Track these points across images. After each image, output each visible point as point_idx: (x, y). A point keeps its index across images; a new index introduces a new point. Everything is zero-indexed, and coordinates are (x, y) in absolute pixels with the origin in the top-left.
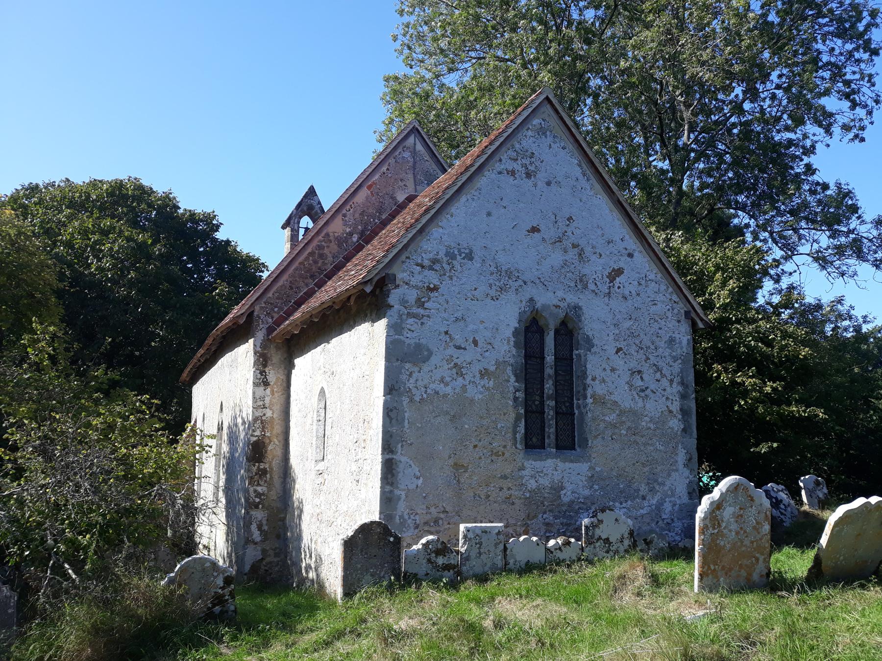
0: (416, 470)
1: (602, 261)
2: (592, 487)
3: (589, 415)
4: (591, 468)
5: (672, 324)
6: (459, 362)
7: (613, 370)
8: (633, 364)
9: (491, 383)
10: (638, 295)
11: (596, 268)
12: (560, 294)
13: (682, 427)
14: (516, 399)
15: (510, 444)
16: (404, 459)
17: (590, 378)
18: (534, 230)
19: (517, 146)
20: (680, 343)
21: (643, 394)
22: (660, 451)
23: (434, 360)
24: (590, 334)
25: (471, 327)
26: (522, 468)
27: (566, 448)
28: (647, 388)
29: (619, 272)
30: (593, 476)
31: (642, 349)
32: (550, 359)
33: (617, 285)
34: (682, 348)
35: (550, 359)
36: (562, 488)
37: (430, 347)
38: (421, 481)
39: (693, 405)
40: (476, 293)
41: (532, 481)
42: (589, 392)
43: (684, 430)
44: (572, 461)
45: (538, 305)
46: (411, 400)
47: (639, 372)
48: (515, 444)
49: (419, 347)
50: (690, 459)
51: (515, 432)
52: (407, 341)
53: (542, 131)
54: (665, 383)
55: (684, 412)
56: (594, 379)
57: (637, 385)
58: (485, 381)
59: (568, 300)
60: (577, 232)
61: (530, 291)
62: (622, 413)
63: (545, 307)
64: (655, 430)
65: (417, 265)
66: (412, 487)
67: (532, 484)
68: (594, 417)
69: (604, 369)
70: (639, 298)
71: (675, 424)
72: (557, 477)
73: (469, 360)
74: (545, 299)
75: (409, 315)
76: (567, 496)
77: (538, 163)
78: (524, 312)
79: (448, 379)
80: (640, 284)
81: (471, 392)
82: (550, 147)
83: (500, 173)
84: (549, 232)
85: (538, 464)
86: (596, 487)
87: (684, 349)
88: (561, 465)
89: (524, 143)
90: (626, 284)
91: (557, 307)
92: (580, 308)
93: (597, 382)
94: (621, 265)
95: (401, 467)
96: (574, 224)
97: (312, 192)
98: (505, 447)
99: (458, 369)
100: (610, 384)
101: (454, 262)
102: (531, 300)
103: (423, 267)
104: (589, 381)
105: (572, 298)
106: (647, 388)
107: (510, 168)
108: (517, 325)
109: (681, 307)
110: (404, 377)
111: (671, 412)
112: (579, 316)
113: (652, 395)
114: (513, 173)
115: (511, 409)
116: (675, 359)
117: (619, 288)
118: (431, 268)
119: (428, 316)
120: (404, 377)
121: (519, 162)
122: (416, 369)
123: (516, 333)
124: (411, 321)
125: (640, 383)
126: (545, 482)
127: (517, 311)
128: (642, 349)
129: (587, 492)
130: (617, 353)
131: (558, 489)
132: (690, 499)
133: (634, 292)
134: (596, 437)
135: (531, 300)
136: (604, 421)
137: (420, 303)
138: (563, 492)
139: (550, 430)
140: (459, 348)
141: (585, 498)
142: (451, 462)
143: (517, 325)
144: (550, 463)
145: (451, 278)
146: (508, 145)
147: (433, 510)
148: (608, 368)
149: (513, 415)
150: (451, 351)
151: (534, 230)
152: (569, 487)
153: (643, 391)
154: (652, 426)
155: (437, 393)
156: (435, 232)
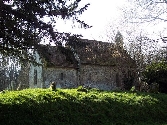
68: (37, 80)
71: (41, 80)
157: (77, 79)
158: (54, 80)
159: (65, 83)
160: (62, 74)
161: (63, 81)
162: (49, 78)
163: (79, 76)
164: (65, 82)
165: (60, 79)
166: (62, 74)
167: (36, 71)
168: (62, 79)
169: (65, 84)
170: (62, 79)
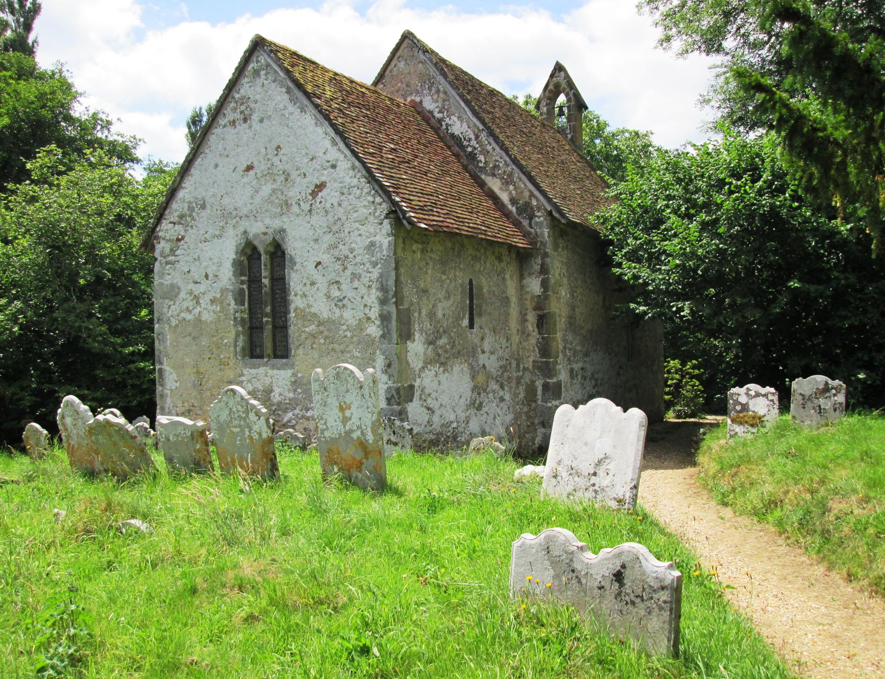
0: (175, 376)
1: (306, 180)
2: (295, 391)
3: (292, 327)
4: (294, 375)
6: (196, 293)
7: (313, 284)
8: (332, 276)
9: (218, 308)
10: (340, 205)
11: (300, 189)
12: (268, 221)
13: (381, 333)
14: (235, 319)
15: (232, 355)
16: (168, 368)
17: (293, 293)
18: (249, 168)
19: (237, 96)
20: (381, 246)
21: (340, 304)
22: (357, 358)
23: (182, 295)
24: (293, 253)
25: (205, 264)
26: (242, 375)
27: (282, 357)
28: (344, 298)
29: (321, 187)
30: (296, 381)
31: (339, 259)
32: (266, 281)
33: (318, 201)
34: (381, 252)
35: (266, 281)
36: (272, 391)
37: (179, 284)
38: (178, 385)
39: (393, 309)
40: (207, 236)
41: (249, 385)
42: (292, 307)
43: (383, 336)
44: (278, 369)
45: (251, 236)
46: (171, 327)
47: (337, 282)
48: (236, 355)
49: (172, 285)
51: (236, 346)
52: (166, 283)
53: (256, 73)
54: (363, 290)
55: (384, 318)
56: (296, 295)
57: (335, 295)
58: (214, 307)
59: (275, 226)
60: (284, 158)
61: (245, 225)
62: (320, 324)
63: (256, 236)
64: (352, 337)
65: (171, 223)
66: (174, 388)
69: (305, 284)
70: (340, 209)
71: (374, 330)
72: (268, 381)
73: (203, 291)
74: (256, 228)
75: (167, 263)
77: (252, 105)
78: (240, 244)
79: (191, 308)
80: (343, 194)
81: (207, 317)
82: (263, 85)
83: (225, 126)
84: (261, 167)
85: (253, 371)
86: (299, 390)
87: (385, 253)
88: (270, 372)
89: (242, 91)
90: (328, 198)
91: (265, 234)
92: (284, 231)
93: (298, 297)
94: (323, 179)
95: (167, 374)
96: (282, 152)
97: (559, 68)
98: (229, 358)
99: (197, 299)
100: (310, 298)
101: (194, 214)
102: (245, 232)
103: (174, 223)
104: (292, 297)
105: (276, 224)
106: (344, 298)
107: (231, 119)
108: (235, 257)
109: (385, 207)
110: (165, 310)
111: (369, 319)
112: (283, 239)
113: (349, 304)
114: (233, 123)
115: (232, 328)
116: (374, 264)
117: (321, 202)
118: (180, 223)
119: (178, 261)
120: (165, 310)
121: (238, 111)
122: (172, 302)
124: (168, 267)
127: (235, 244)
128: (339, 259)
129: (291, 395)
130: (316, 267)
131: (269, 391)
132: (389, 404)
133: (335, 204)
134: (297, 348)
135: (245, 232)
136: (304, 332)
137: (173, 252)
138: (272, 394)
140: (196, 283)
141: (290, 400)
142: (195, 370)
143: (235, 257)
144: (262, 370)
145: (192, 227)
146: (229, 99)
147: (186, 404)
148: (308, 286)
149: (234, 333)
150: (191, 286)
151: (249, 168)
152: (277, 390)
153: (341, 300)
154: (349, 334)
155: (184, 319)
156: (181, 194)
157: (523, 320)
158: (445, 332)
159: (483, 352)
160: (471, 282)
161: (473, 336)
162: (424, 312)
163: (529, 304)
164: (482, 339)
165: (466, 322)
166: (471, 282)
167: (278, 253)
168: (471, 326)
169: (483, 359)
170: (471, 326)
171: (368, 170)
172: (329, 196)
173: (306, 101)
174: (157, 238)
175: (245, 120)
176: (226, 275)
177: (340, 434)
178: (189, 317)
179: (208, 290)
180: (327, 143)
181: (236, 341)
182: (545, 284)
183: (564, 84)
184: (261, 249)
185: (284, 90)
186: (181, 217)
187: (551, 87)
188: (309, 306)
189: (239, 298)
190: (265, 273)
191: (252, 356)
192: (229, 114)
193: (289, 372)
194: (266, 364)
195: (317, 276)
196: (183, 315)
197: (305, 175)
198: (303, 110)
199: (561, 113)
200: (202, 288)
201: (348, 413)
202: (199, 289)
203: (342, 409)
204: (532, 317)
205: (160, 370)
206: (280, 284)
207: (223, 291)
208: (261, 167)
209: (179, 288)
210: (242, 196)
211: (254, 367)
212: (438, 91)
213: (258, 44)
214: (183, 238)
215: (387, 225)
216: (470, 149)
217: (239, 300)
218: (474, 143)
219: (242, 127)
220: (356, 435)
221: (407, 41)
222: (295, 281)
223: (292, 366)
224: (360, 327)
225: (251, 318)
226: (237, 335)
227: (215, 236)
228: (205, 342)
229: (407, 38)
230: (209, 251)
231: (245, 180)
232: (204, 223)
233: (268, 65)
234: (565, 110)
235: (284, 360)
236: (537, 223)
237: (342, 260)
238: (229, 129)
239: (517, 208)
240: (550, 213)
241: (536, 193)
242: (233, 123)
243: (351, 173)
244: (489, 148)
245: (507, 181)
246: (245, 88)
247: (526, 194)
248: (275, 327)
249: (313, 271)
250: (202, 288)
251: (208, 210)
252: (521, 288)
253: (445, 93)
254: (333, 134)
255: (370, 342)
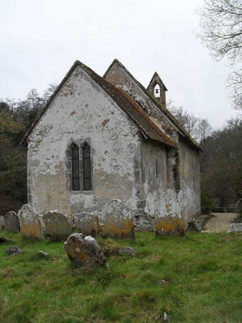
0: (37, 198)
5: (130, 137)
8: (113, 157)
12: (82, 134)
13: (135, 179)
18: (73, 113)
23: (41, 164)
29: (107, 121)
32: (81, 159)
35: (81, 159)
42: (94, 169)
49: (36, 160)
50: (138, 192)
53: (77, 75)
55: (136, 174)
60: (90, 109)
62: (107, 176)
63: (77, 140)
67: (73, 202)
68: (96, 178)
71: (132, 178)
74: (76, 137)
75: (33, 151)
76: (86, 207)
77: (75, 88)
84: (79, 113)
88: (83, 196)
89: (70, 83)
91: (81, 139)
92: (90, 139)
94: (108, 118)
95: (33, 197)
97: (156, 75)
105: (86, 136)
109: (136, 130)
111: (129, 174)
123: (67, 152)
124: (34, 153)
125: (115, 164)
126: (77, 201)
131: (82, 204)
132: (138, 208)
135: (72, 139)
139: (82, 185)
144: (79, 195)
149: (66, 181)
150: (46, 161)
151: (73, 113)
155: (42, 174)
163: (171, 169)
167: (86, 147)
171: (128, 114)
172: (110, 124)
173: (100, 87)
174: (29, 141)
175: (71, 94)
176: (63, 156)
177: (166, 216)
178: (44, 173)
179: (54, 162)
180: (110, 104)
181: (67, 183)
182: (177, 161)
183: (158, 81)
184: (79, 145)
185: (89, 82)
186: (41, 132)
187: (153, 82)
188: (102, 169)
189: (68, 166)
190: (80, 156)
191: (74, 190)
192: (65, 90)
193: (92, 196)
194: (81, 193)
195: (105, 157)
196: (42, 172)
197: (99, 116)
198: (98, 90)
199: (157, 92)
200: (51, 161)
201: (170, 208)
202: (48, 162)
203: (167, 206)
204: (171, 173)
205: (30, 196)
206: (88, 161)
207: (61, 163)
208: (79, 113)
209: (39, 162)
210: (70, 125)
211: (76, 194)
212: (129, 83)
213: (78, 64)
214: (41, 141)
215: (137, 137)
216: (144, 107)
217: (68, 167)
218: (145, 104)
219: (69, 97)
220: (173, 216)
221: (115, 64)
222: (95, 159)
223: (93, 194)
224: (126, 177)
225: (73, 174)
226: (67, 181)
227: (57, 140)
228: (52, 183)
229: (116, 61)
230: (53, 146)
231: (71, 117)
232: (52, 134)
233: (82, 73)
234: (159, 91)
235: (89, 191)
236: (174, 137)
237: (118, 151)
238: (64, 97)
239: (165, 131)
240: (178, 133)
241: (172, 124)
242: (66, 95)
243: (121, 116)
244: (152, 106)
245: (160, 119)
246: (72, 81)
247: (168, 125)
248: (84, 178)
249: (104, 155)
250: (51, 161)
251: (53, 130)
252: (167, 162)
253: (133, 84)
254: (112, 100)
255: (130, 183)
